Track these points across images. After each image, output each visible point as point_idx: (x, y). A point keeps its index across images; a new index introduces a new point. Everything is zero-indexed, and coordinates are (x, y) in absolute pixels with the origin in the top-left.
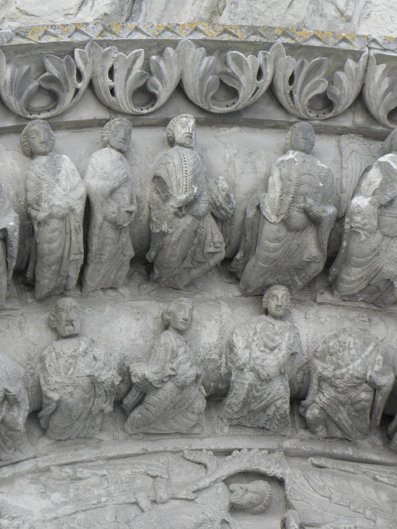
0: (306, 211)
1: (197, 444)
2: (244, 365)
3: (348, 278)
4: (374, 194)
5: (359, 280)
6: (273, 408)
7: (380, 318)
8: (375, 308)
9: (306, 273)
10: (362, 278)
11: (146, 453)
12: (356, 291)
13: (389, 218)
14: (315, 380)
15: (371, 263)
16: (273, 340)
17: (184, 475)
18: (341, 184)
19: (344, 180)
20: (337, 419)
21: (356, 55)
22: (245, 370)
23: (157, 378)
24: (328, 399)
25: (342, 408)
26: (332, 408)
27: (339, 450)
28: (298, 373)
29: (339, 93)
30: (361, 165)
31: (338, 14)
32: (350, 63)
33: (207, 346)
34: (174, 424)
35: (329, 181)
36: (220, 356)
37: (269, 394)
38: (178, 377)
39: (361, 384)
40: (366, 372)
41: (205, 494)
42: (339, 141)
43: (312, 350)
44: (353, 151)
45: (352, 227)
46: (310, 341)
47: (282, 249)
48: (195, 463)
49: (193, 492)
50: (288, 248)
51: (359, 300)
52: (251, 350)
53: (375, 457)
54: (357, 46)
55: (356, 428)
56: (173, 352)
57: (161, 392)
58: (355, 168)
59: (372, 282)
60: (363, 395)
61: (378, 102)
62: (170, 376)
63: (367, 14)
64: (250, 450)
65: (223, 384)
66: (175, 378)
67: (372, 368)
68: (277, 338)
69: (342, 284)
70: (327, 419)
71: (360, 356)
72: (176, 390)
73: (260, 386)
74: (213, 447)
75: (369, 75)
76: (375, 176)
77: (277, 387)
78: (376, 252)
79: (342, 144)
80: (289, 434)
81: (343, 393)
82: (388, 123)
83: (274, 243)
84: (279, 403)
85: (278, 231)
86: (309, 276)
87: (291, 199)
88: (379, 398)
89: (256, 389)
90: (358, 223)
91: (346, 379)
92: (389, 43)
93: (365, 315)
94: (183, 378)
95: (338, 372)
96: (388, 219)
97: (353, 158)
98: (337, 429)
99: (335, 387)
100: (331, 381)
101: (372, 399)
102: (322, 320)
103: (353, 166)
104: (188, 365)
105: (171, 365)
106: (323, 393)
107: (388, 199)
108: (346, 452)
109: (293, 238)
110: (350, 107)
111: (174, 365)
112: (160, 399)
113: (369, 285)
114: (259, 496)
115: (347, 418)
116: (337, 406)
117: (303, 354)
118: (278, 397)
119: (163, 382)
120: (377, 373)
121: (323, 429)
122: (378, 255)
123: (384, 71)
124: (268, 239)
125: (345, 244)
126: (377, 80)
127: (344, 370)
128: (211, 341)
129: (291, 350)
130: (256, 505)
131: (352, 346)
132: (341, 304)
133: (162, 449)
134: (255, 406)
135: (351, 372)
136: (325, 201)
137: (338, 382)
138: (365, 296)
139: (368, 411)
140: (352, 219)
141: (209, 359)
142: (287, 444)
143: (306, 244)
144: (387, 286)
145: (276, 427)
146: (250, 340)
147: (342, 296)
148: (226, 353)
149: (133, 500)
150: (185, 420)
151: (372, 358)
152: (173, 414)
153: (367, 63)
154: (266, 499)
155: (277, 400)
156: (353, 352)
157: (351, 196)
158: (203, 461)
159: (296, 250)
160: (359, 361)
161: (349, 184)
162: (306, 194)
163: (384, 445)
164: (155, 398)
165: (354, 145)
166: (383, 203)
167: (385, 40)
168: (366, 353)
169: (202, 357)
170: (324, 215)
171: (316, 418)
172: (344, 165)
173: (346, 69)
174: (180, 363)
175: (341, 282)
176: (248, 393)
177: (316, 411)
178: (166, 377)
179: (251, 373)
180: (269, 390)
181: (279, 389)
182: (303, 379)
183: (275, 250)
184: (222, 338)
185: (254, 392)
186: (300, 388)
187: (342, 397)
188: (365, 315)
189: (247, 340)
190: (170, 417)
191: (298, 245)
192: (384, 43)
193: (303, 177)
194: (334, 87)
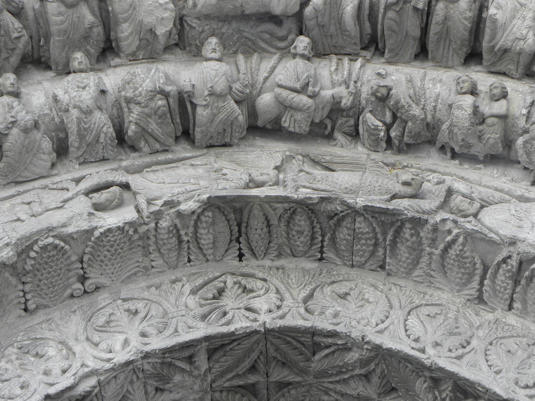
1: (56, 179)
2: (68, 105)
6: (102, 135)
8: (153, 60)
9: (93, 39)
10: (132, 33)
11: (19, 194)
14: (124, 104)
15: (133, 17)
16: (82, 82)
17: (52, 199)
20: (150, 130)
22: (70, 109)
23: (2, 127)
24: (137, 115)
25: (150, 120)
26: (143, 121)
27: (162, 157)
28: (112, 109)
33: (38, 106)
34: (34, 169)
36: (51, 110)
37: (95, 124)
38: (19, 122)
39: (155, 95)
40: (156, 86)
41: (71, 203)
43: (116, 90)
46: (113, 85)
47: (68, 22)
48: (59, 190)
49: (61, 202)
50: (72, 21)
51: (140, 58)
52: (69, 93)
53: (188, 155)
55: (166, 133)
56: (9, 105)
57: (10, 137)
59: (141, 36)
60: (160, 103)
62: (13, 123)
64: (98, 173)
65: (61, 132)
66: (17, 124)
67: (159, 82)
68: (85, 80)
69: (122, 43)
70: (144, 133)
71: (148, 77)
72: (22, 134)
73: (86, 118)
74: (70, 178)
77: (99, 116)
80: (124, 158)
81: (146, 106)
83: (59, 17)
84: (104, 129)
85: (58, 7)
86: (96, 41)
88: (171, 100)
89: (83, 121)
91: (143, 95)
94: (23, 122)
95: (137, 92)
98: (155, 142)
99: (138, 103)
100: (135, 100)
101: (167, 104)
102: (119, 73)
104: (24, 112)
105: (10, 114)
106: (132, 112)
108: (168, 157)
109: (73, 13)
111: (13, 114)
112: (11, 143)
114: (112, 194)
115: (157, 127)
116: (146, 119)
117: (111, 95)
118: (102, 125)
119: (9, 128)
120: (163, 84)
121: (145, 144)
122: (134, 9)
124: (53, 15)
125: (110, 9)
127: (140, 89)
128: (41, 102)
129: (98, 87)
130: (112, 201)
131: (140, 73)
133: (30, 188)
134: (89, 138)
135: (145, 88)
137: (139, 99)
139: (168, 115)
141: (43, 114)
142: (124, 164)
143: (83, 14)
144: (153, 37)
145: (112, 153)
146: (66, 87)
147: (127, 56)
148: (54, 107)
149: (15, 218)
150: (40, 161)
151: (156, 76)
152: (30, 158)
154: (118, 194)
155: (103, 127)
156: (142, 76)
158: (65, 187)
159: (78, 21)
160: (148, 80)
163: (192, 148)
164: (8, 144)
168: (152, 74)
169: (37, 114)
171: (135, 133)
174: (17, 112)
175: (121, 41)
176: (79, 126)
177: (133, 127)
178: (10, 123)
179: (75, 110)
180: (93, 121)
181: (100, 118)
182: (118, 114)
183: (62, 22)
184: (48, 98)
185: (83, 124)
186: (119, 122)
187: (146, 110)
189: (64, 89)
190: (28, 161)
191: (78, 17)
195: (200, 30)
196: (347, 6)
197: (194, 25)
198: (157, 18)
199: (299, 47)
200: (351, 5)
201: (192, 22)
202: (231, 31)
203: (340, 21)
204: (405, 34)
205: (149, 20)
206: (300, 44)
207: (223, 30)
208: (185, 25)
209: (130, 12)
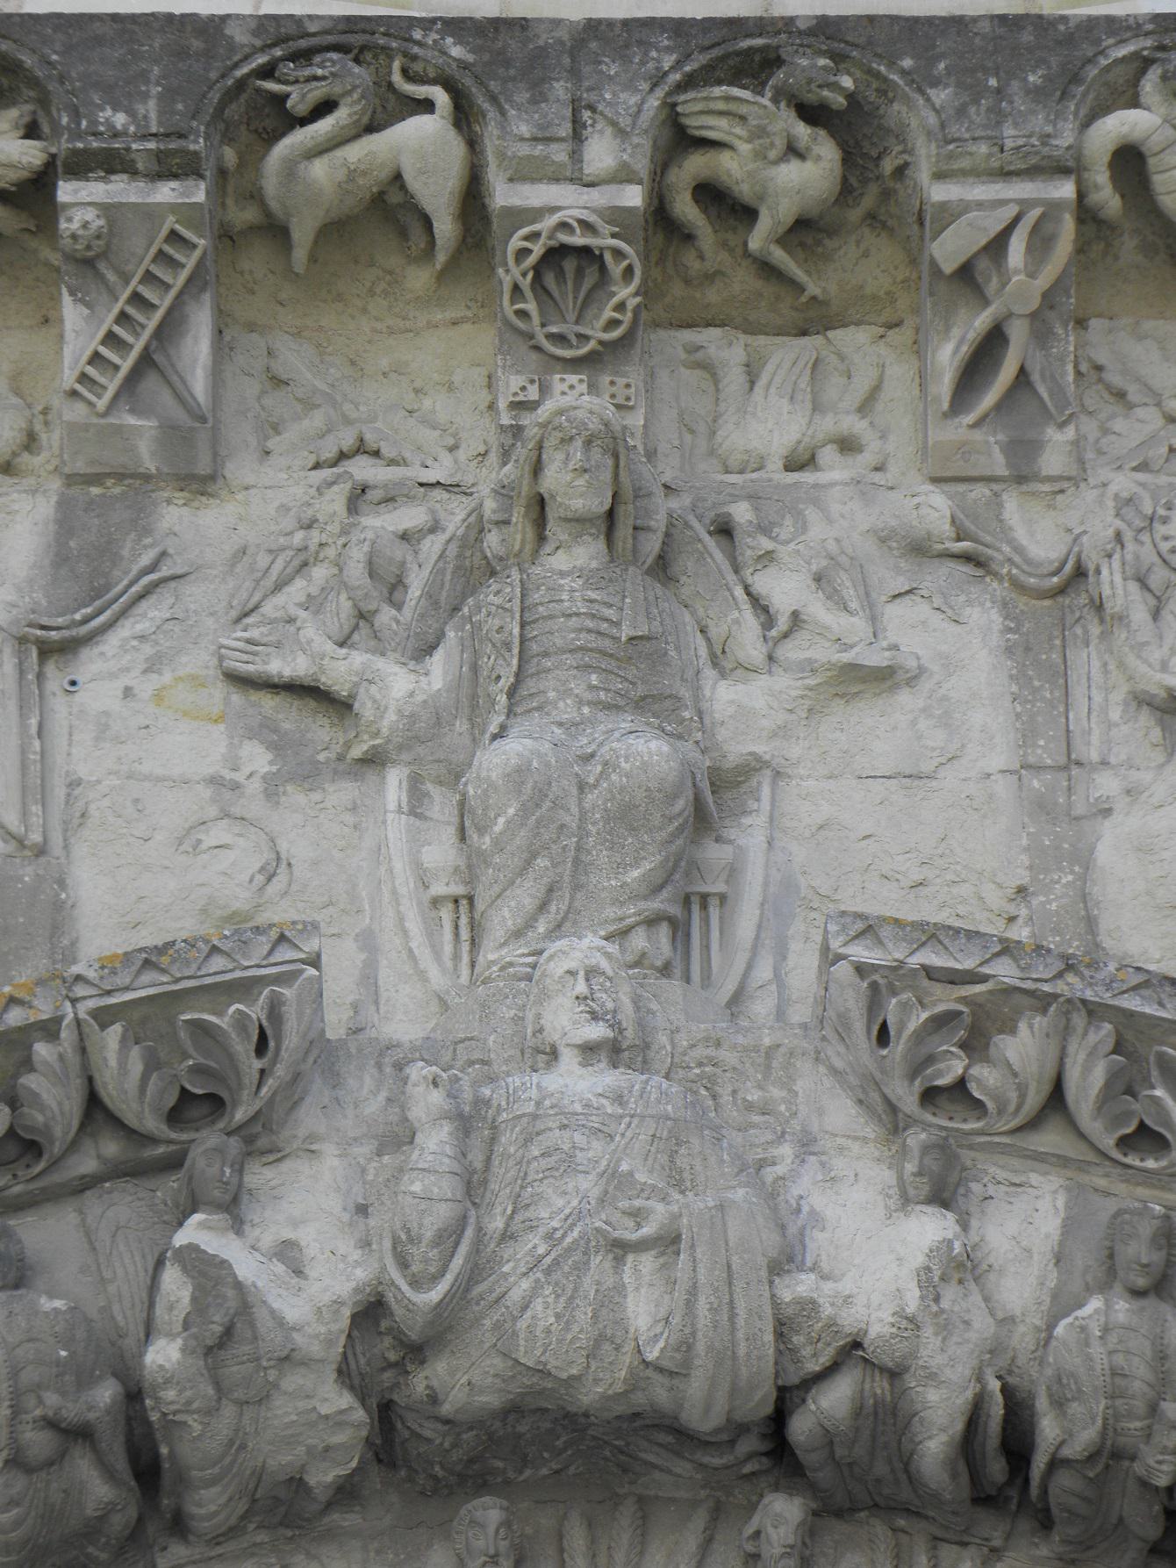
0: (51, 1424)
3: (203, 1511)
4: (186, 1325)
5: (226, 1505)
7: (308, 1554)
8: (289, 1533)
10: (230, 1499)
12: (233, 1521)
13: (235, 1369)
18: (113, 1318)
19: (116, 1308)
21: (49, 1029)
29: (40, 1118)
30: (144, 1257)
31: (11, 847)
32: (42, 1050)
35: (80, 1334)
42: (81, 1212)
44: (118, 1229)
45: (165, 1414)
54: (43, 1009)
58: (131, 1269)
59: (258, 1496)
61: (135, 1106)
63: (78, 814)
75: (94, 1057)
76: (176, 1286)
78: (237, 1444)
79: (89, 1220)
82: (173, 1135)
87: (8, 1412)
90: (172, 1403)
92: (114, 972)
93: (273, 1560)
96: (234, 1372)
97: (122, 1247)
103: (128, 1268)
107: (218, 1329)
110: (82, 1126)
113: (254, 1501)
122: (243, 1447)
123: (123, 1040)
125: (164, 1450)
126: (113, 1063)
132: (213, 1554)
136: (85, 1380)
138: (258, 1518)
140: (157, 1399)
153: (80, 1034)
157: (142, 1335)
161: (129, 1313)
162: (39, 1386)
165: (120, 1209)
166: (209, 1342)
167: (102, 968)
170: (91, 1416)
172: (107, 1275)
173: (38, 1066)
188: (273, 1560)
192: (102, 978)
193: (19, 1352)
194: (25, 1110)
195: (447, 1445)
196: (930, 1438)
197: (427, 1433)
198: (310, 1451)
199: (769, 1542)
200: (944, 1438)
201: (421, 1426)
202: (548, 1425)
203: (905, 1463)
204: (1114, 1521)
205: (282, 1460)
206: (770, 1530)
207: (522, 1429)
208: (399, 1425)
209: (228, 1459)
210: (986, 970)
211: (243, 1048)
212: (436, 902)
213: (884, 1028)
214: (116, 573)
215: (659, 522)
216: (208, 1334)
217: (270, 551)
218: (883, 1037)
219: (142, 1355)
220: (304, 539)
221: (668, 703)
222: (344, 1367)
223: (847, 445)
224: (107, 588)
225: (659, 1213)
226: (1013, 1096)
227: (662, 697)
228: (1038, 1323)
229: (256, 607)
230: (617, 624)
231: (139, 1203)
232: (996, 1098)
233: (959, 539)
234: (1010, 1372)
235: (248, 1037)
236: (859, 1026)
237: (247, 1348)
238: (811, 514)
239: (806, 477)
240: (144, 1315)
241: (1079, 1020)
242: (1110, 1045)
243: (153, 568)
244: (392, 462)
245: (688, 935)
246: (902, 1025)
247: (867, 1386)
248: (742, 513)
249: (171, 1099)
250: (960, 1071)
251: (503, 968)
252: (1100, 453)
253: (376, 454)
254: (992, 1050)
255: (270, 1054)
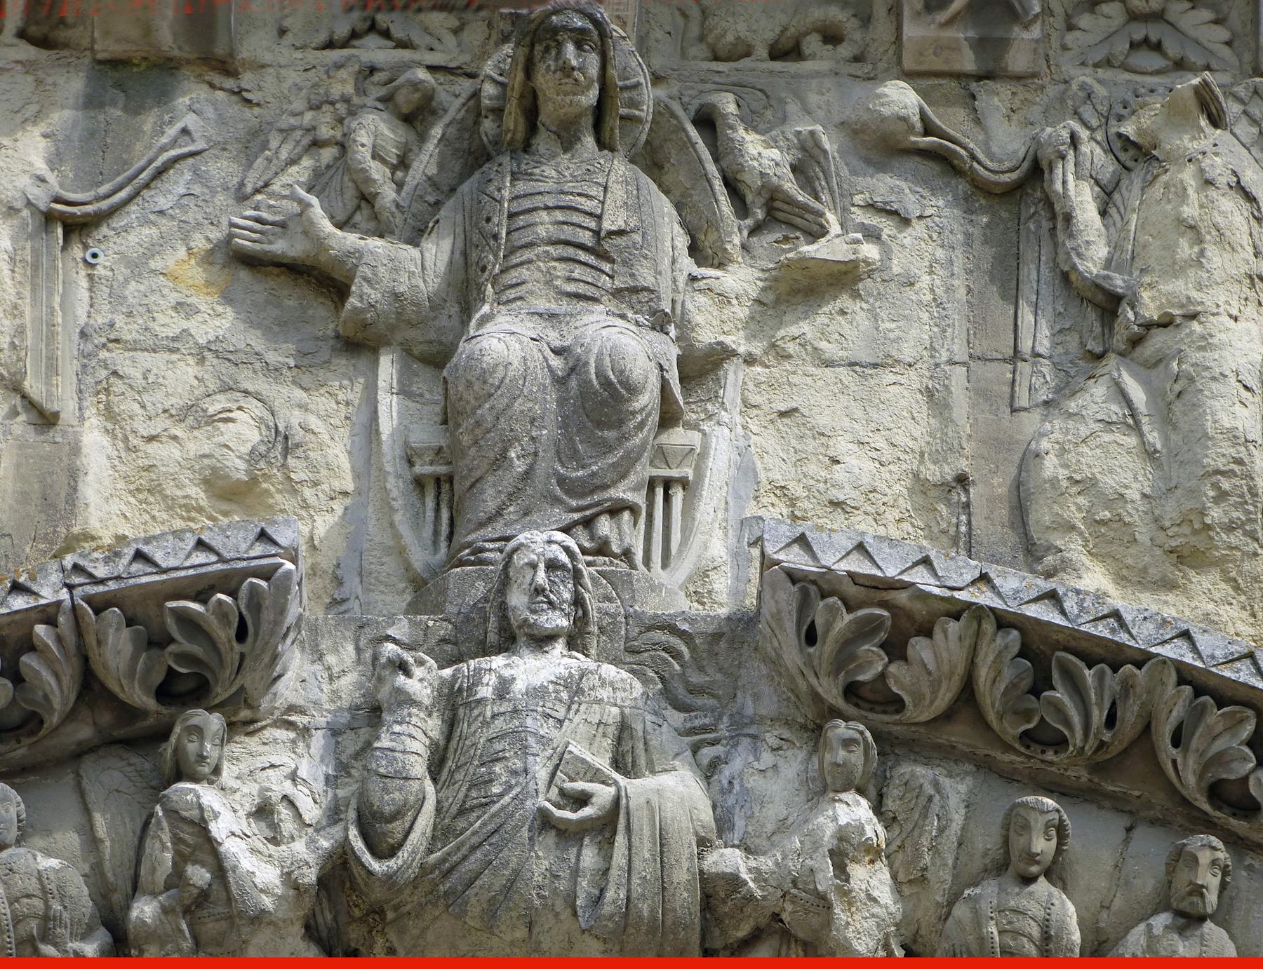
157: (129, 890)
210: (905, 578)
211: (224, 634)
212: (419, 483)
213: (812, 628)
214: (139, 147)
215: (646, 111)
216: (186, 895)
217: (281, 131)
218: (811, 637)
219: (128, 908)
220: (313, 119)
221: (644, 296)
222: (312, 922)
223: (832, 37)
224: (126, 164)
225: (603, 794)
226: (926, 690)
227: (635, 290)
228: (939, 899)
229: (266, 185)
230: (599, 217)
231: (130, 769)
232: (910, 693)
233: (927, 133)
234: (915, 941)
235: (229, 624)
236: (790, 625)
237: (221, 909)
238: (793, 108)
239: (792, 67)
240: (132, 871)
241: (989, 626)
242: (1015, 649)
243: (174, 143)
244: (403, 45)
245: (650, 516)
246: (829, 626)
247: (783, 953)
248: (728, 105)
249: (158, 678)
250: (880, 669)
251: (472, 554)
252: (1065, 48)
253: (386, 34)
254: (910, 652)
255: (250, 639)
